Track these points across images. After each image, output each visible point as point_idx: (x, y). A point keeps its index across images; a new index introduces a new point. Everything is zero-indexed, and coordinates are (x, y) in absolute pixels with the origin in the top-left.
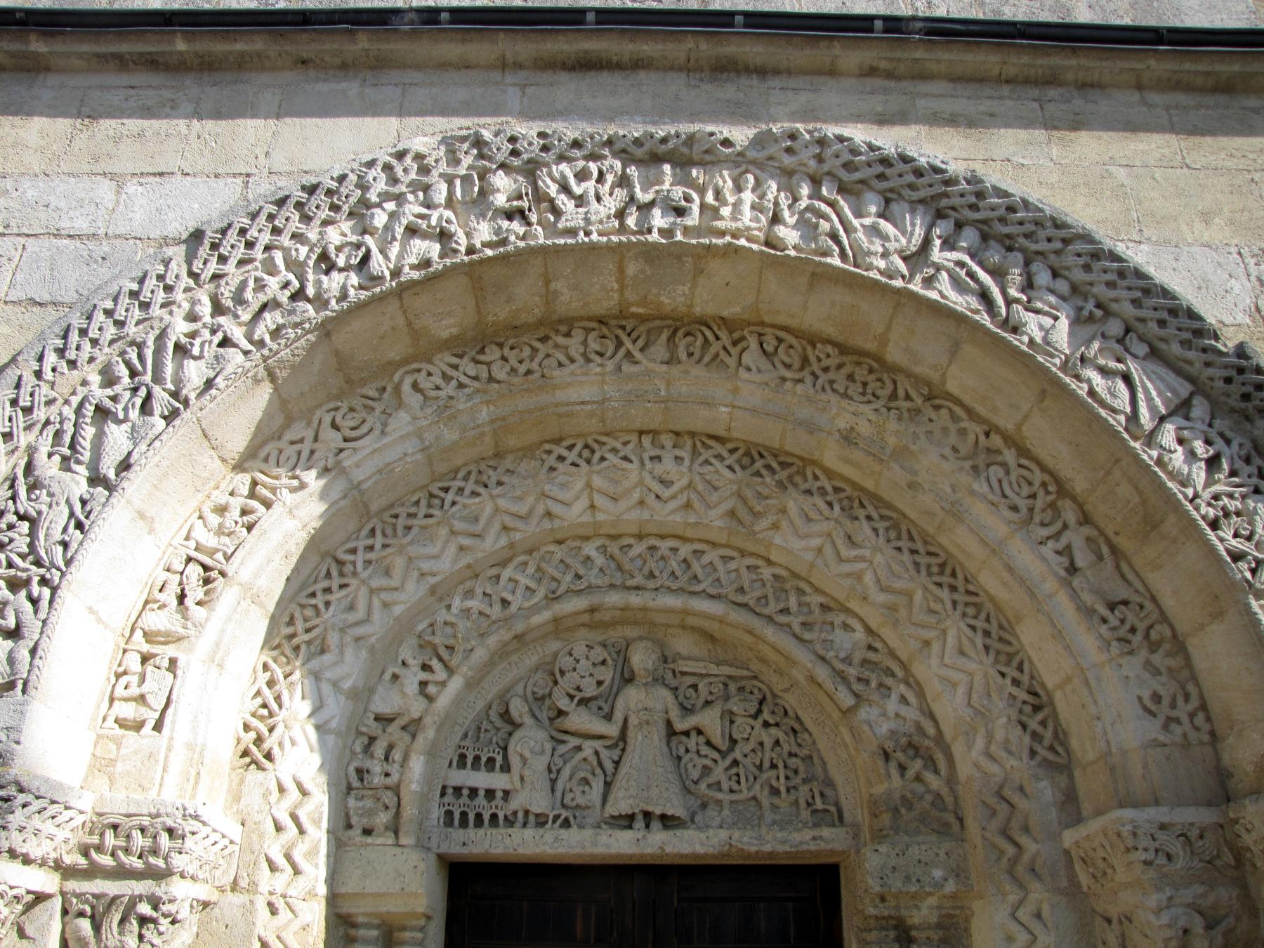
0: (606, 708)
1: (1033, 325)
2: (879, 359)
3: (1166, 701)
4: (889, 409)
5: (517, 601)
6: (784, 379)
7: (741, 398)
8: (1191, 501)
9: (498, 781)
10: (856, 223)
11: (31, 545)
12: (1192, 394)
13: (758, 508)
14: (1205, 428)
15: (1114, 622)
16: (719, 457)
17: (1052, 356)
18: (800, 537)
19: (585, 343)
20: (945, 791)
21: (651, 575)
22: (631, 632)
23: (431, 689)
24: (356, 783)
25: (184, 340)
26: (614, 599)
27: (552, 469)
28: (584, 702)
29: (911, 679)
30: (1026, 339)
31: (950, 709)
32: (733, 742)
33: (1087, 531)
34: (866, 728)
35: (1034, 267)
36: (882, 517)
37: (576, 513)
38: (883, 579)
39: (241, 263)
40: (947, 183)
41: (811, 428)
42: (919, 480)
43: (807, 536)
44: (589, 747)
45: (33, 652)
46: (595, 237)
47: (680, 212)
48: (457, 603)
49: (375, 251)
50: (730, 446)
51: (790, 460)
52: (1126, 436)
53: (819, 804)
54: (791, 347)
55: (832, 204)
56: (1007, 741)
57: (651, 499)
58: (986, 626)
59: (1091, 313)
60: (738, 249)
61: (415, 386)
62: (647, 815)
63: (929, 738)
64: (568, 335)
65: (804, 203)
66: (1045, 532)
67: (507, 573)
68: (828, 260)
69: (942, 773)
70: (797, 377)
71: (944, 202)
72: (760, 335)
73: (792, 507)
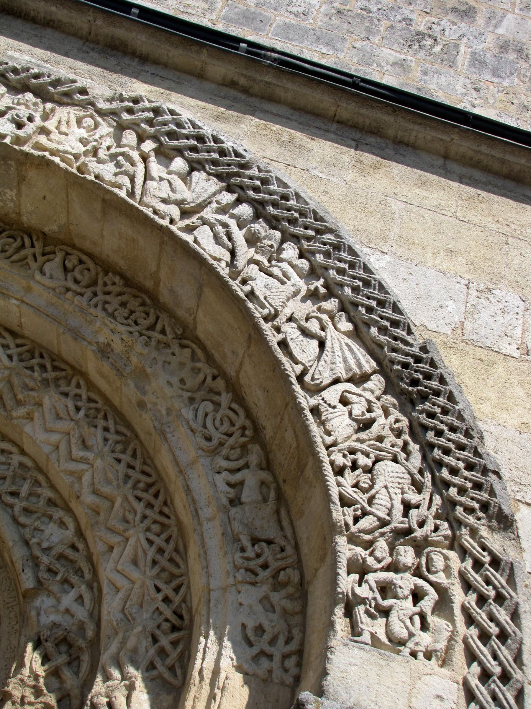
2: (154, 298)
3: (267, 637)
4: (141, 335)
6: (68, 290)
8: (327, 448)
12: (374, 372)
13: (20, 396)
15: (250, 553)
17: (263, 307)
29: (95, 584)
33: (264, 475)
34: (33, 613)
35: (285, 246)
36: (118, 432)
38: (96, 481)
40: (245, 166)
41: (77, 335)
42: (145, 399)
43: (48, 431)
50: (19, 341)
51: (63, 366)
54: (88, 270)
56: (135, 651)
58: (163, 544)
59: (316, 288)
60: (49, 163)
63: (84, 638)
66: (225, 464)
68: (116, 191)
69: (81, 675)
70: (79, 290)
71: (235, 180)
72: (67, 254)
73: (47, 401)
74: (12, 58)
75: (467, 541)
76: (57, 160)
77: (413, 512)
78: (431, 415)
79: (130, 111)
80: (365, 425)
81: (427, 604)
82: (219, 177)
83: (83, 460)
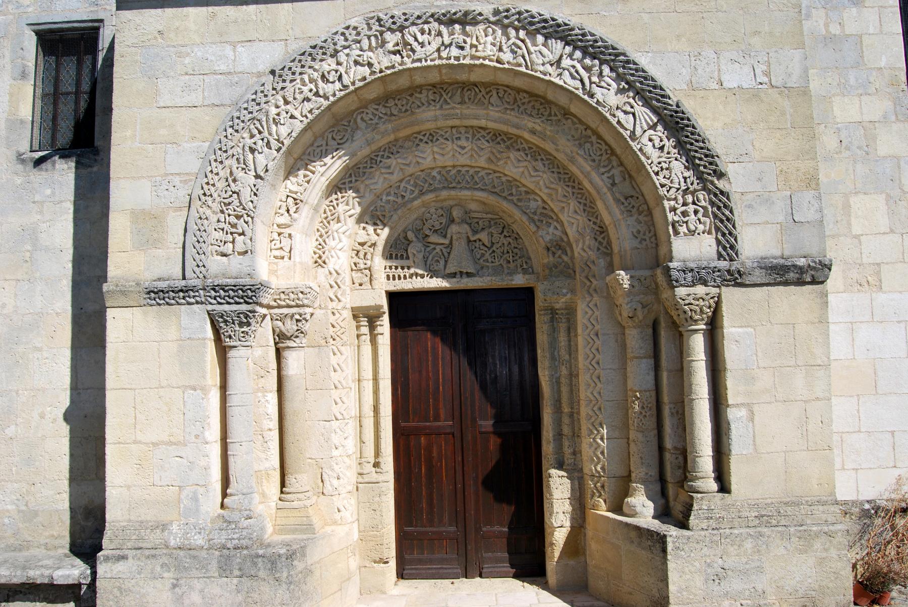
1: (599, 93)
5: (408, 196)
6: (506, 109)
7: (490, 116)
10: (532, 49)
11: (240, 202)
14: (661, 135)
15: (626, 204)
16: (484, 137)
18: (514, 167)
19: (427, 96)
20: (569, 262)
21: (459, 182)
22: (451, 203)
24: (354, 268)
25: (276, 117)
26: (444, 194)
27: (418, 145)
28: (435, 231)
30: (595, 100)
31: (571, 232)
33: (621, 168)
36: (547, 159)
37: (428, 162)
39: (292, 81)
44: (438, 248)
45: (251, 239)
46: (429, 63)
47: (462, 48)
48: (384, 198)
49: (343, 73)
52: (629, 139)
53: (525, 267)
55: (523, 41)
57: (457, 155)
61: (362, 118)
64: (420, 93)
65: (511, 42)
66: (603, 170)
67: (403, 185)
73: (511, 155)
74: (437, 6)
75: (710, 187)
76: (487, 62)
77: (688, 180)
78: (687, 137)
79: (507, 17)
80: (662, 148)
81: (700, 215)
82: (561, 39)
83: (537, 176)
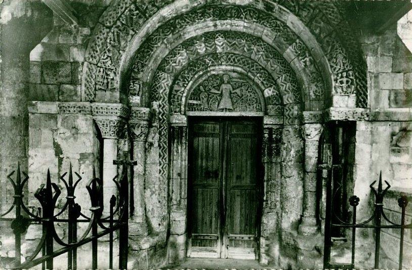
0: (218, 88)
9: (199, 102)
15: (311, 76)
23: (185, 85)
32: (242, 95)
53: (257, 108)
62: (226, 109)
